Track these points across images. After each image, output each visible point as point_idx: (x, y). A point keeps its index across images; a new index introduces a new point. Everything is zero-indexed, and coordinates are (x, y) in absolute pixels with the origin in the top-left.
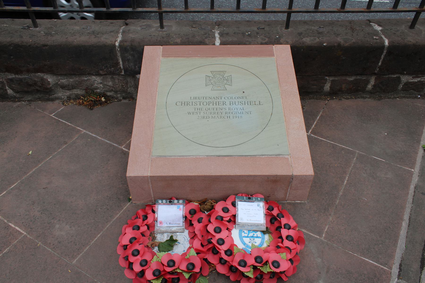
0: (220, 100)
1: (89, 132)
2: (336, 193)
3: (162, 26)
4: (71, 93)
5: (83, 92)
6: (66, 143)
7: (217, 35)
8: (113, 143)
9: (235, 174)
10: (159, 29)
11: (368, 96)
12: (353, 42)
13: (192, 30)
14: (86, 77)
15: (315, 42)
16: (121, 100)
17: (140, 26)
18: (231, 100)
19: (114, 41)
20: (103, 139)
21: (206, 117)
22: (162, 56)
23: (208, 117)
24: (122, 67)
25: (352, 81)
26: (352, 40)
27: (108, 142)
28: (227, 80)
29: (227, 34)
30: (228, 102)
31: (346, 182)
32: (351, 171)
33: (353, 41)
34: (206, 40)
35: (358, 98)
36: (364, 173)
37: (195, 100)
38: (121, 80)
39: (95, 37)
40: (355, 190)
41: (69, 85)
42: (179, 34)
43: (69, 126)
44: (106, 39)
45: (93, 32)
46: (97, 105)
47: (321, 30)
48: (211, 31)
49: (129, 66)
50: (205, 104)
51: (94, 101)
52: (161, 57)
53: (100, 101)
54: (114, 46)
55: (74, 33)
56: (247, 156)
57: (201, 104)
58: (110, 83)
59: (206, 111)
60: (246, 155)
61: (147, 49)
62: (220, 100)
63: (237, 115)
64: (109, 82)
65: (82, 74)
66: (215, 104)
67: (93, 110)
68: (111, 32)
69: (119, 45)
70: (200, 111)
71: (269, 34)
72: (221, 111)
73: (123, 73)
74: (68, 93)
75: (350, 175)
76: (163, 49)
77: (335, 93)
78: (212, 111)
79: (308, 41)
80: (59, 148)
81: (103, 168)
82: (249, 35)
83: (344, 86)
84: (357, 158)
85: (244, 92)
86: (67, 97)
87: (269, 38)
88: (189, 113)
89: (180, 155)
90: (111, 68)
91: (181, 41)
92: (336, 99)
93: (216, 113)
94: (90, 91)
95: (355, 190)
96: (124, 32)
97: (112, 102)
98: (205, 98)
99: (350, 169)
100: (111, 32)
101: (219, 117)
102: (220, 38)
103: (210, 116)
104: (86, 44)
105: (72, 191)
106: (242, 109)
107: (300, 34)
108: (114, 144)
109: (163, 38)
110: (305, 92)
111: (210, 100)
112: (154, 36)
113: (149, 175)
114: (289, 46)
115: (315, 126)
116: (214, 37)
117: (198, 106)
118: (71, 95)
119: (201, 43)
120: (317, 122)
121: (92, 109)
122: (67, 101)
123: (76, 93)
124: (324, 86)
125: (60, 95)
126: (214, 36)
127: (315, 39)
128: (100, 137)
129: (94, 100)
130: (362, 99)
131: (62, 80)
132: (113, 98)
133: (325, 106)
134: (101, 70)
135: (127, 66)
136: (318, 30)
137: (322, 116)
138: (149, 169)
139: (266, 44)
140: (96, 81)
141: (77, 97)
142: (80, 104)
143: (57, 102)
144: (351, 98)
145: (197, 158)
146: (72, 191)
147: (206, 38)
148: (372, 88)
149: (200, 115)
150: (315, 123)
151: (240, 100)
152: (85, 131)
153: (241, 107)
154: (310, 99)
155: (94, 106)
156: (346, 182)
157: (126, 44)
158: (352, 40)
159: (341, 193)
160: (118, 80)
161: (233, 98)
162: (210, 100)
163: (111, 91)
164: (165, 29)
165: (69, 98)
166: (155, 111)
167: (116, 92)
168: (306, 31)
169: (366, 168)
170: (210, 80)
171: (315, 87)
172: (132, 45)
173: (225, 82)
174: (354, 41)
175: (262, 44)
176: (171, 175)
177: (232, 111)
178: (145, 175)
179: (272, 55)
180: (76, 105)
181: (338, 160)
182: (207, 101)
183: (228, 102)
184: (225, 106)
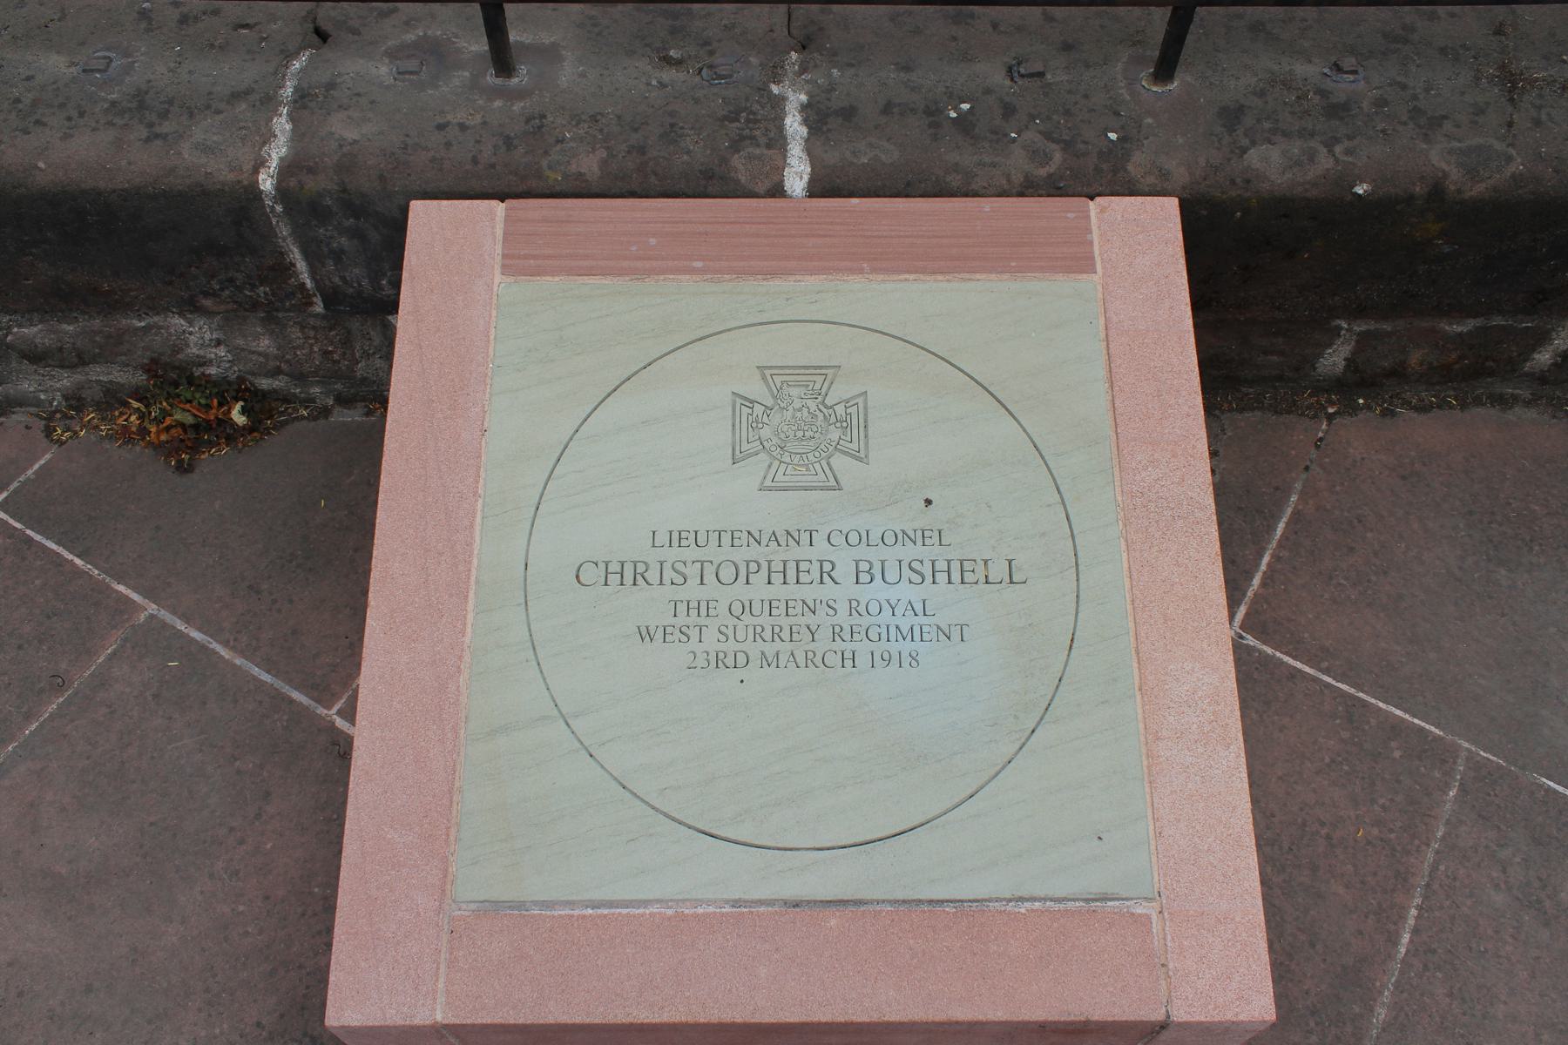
0: (803, 552)
1: (174, 613)
2: (1357, 1009)
3: (502, 58)
4: (78, 378)
5: (140, 378)
6: (61, 687)
7: (794, 125)
8: (290, 682)
9: (875, 1017)
10: (491, 79)
11: (1525, 394)
12: (1513, 176)
13: (662, 85)
14: (140, 319)
15: (1310, 176)
16: (326, 412)
17: (393, 55)
18: (862, 552)
19: (247, 167)
20: (238, 661)
21: (730, 661)
22: (506, 270)
23: (741, 659)
24: (309, 284)
25: (1460, 335)
26: (1509, 159)
27: (266, 677)
28: (845, 424)
29: (848, 113)
30: (844, 571)
31: (1406, 938)
32: (1434, 868)
33: (1512, 169)
34: (739, 166)
35: (1478, 402)
36: (1497, 886)
37: (672, 554)
38: (314, 328)
39: (148, 140)
40: (1450, 995)
41: (61, 349)
42: (594, 119)
43: (78, 573)
44: (206, 149)
45: (140, 102)
46: (211, 444)
47: (1343, 87)
48: (763, 89)
49: (343, 278)
50: (727, 573)
51: (196, 427)
52: (497, 270)
53: (226, 422)
54: (254, 193)
55: (35, 103)
56: (943, 901)
57: (710, 577)
58: (265, 344)
59: (732, 621)
60: (935, 897)
61: (424, 217)
62: (803, 552)
63: (894, 647)
64: (257, 338)
65: (112, 304)
66: (777, 578)
67: (195, 476)
68: (236, 96)
69: (278, 188)
70: (703, 621)
71: (1067, 113)
72: (809, 619)
73: (319, 308)
74: (65, 380)
75: (1426, 898)
76: (507, 219)
77: (1364, 385)
78: (765, 620)
79: (1274, 165)
80: (28, 717)
81: (242, 842)
82: (963, 123)
83: (1415, 358)
84: (1463, 789)
85: (928, 502)
86: (66, 397)
87: (1067, 146)
88: (645, 634)
89: (597, 895)
90: (253, 287)
91: (604, 163)
92: (1368, 407)
93: (785, 635)
94: (171, 377)
95: (1450, 995)
96: (302, 98)
97: (283, 424)
98: (726, 539)
99: (1430, 856)
100: (236, 96)
101: (801, 660)
102: (809, 150)
103: (754, 650)
104: (102, 185)
105: (89, 989)
106: (919, 607)
107: (1231, 116)
108: (296, 695)
109: (509, 142)
110: (1222, 381)
111: (755, 552)
112: (463, 127)
113: (439, 1017)
114: (1172, 203)
115: (1264, 584)
116: (778, 142)
117: (692, 591)
118: (80, 387)
119: (710, 183)
120: (1276, 558)
121: (183, 469)
122: (66, 416)
123: (104, 378)
124: (1321, 355)
125: (27, 386)
126: (781, 128)
127: (1312, 159)
128: (226, 644)
129: (194, 420)
130: (1493, 412)
131: (20, 326)
132: (286, 400)
133: (1314, 454)
134: (206, 295)
135: (337, 280)
136: (1329, 85)
137: (1297, 516)
138: (441, 985)
139: (1055, 188)
140: (198, 338)
141: (112, 399)
142: (125, 435)
143: (19, 417)
144: (1443, 405)
145: (683, 918)
146: (89, 989)
147: (736, 146)
148: (1555, 364)
149: (699, 648)
150: (1263, 567)
151: (909, 552)
152: (152, 608)
153: (914, 594)
154: (1241, 410)
155: (194, 449)
156: (1406, 938)
157: (313, 184)
158: (1509, 159)
159: (1381, 1014)
160: (303, 328)
161: (875, 537)
162: (755, 552)
163: (277, 372)
164: (522, 76)
165: (76, 402)
166: (470, 616)
167: (300, 378)
168: (1261, 94)
169: (1504, 854)
170: (755, 425)
171: (1275, 358)
172: (344, 191)
173: (835, 434)
174: (1517, 167)
175: (1028, 188)
176: (551, 1020)
177: (866, 621)
178: (422, 1018)
179: (1083, 264)
180: (109, 437)
181: (1373, 801)
182: (740, 555)
183: (844, 571)
184: (828, 591)
